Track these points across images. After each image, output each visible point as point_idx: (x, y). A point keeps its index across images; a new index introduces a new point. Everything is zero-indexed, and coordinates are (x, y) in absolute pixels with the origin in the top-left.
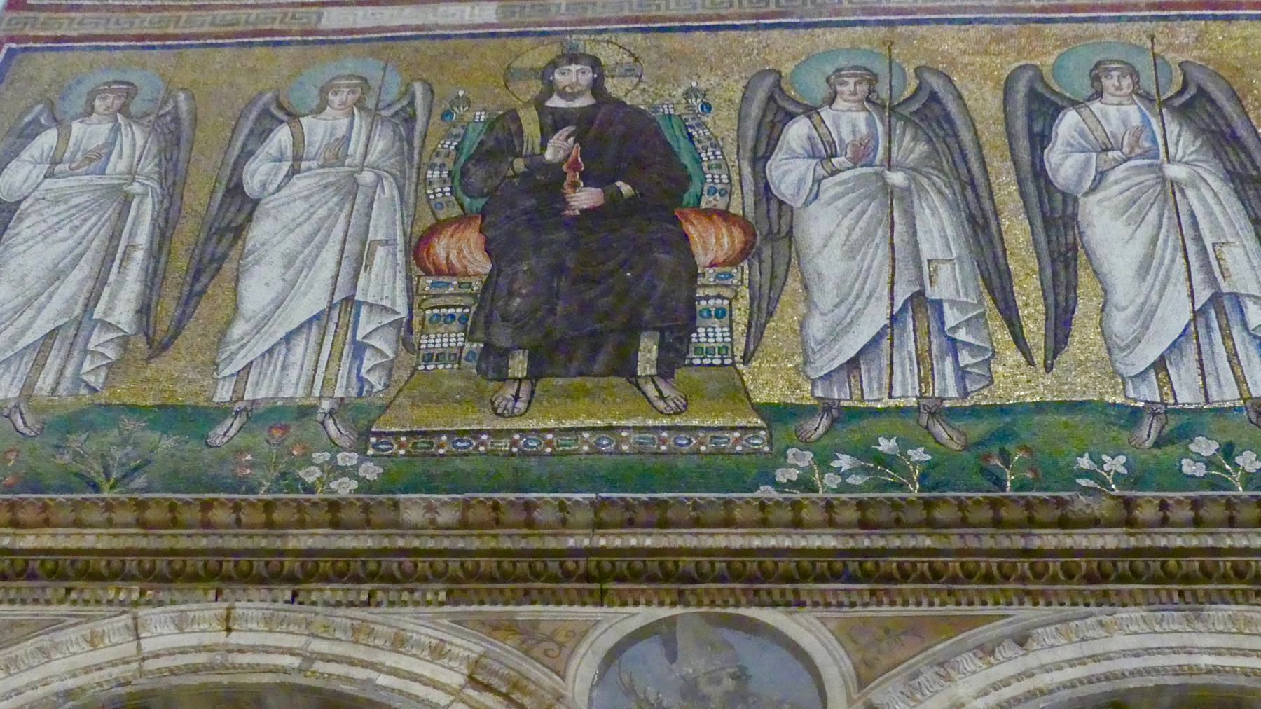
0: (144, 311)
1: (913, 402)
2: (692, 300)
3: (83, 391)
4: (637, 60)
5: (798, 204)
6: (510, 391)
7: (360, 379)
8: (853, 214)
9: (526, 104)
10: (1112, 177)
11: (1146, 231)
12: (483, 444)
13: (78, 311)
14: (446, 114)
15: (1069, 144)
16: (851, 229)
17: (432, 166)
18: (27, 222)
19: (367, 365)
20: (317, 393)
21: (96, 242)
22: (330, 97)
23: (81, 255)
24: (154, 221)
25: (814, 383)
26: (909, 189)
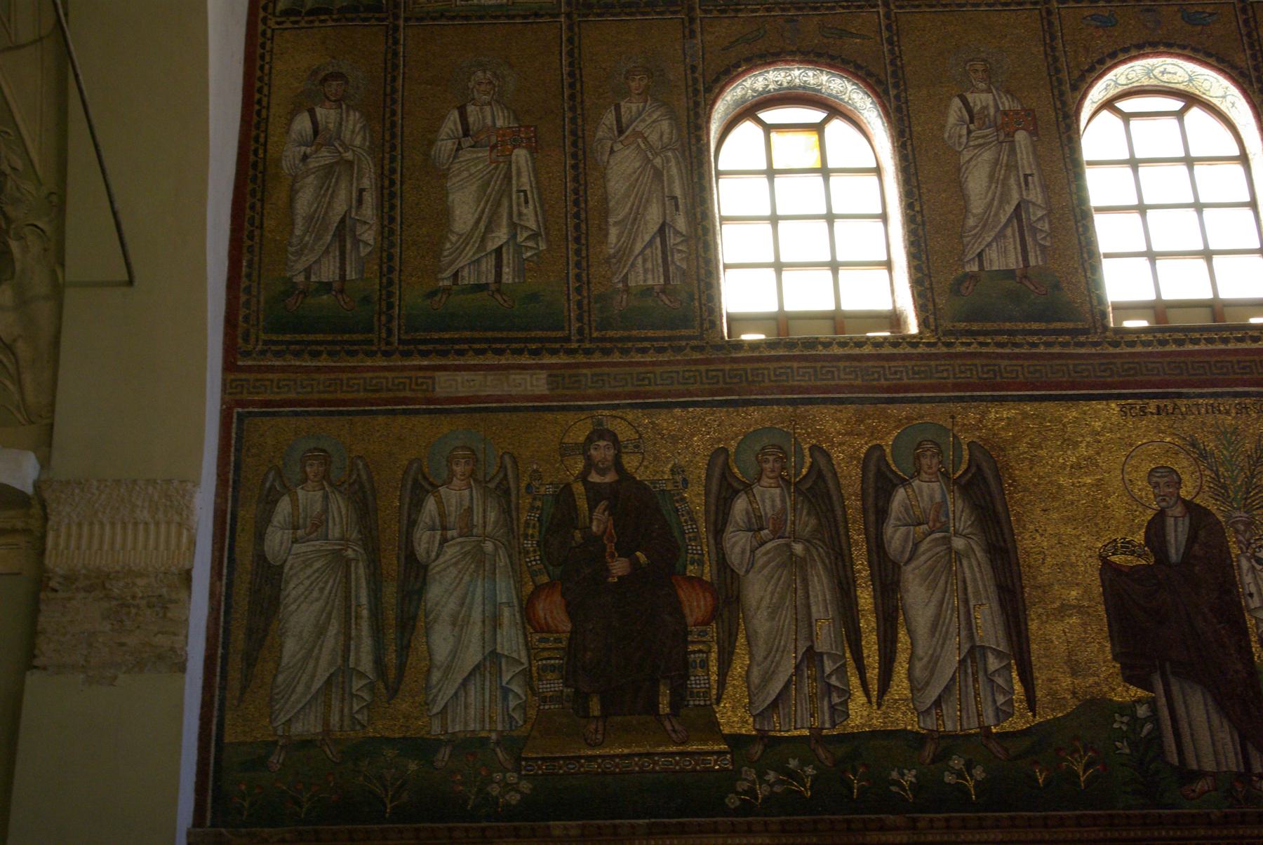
0: (378, 662)
1: (807, 733)
2: (687, 653)
3: (358, 727)
4: (640, 437)
5: (742, 573)
6: (592, 727)
7: (511, 717)
8: (773, 581)
9: (575, 481)
10: (924, 546)
11: (937, 595)
12: (582, 766)
13: (340, 661)
14: (529, 486)
15: (899, 519)
16: (772, 593)
17: (526, 536)
18: (292, 585)
19: (512, 704)
20: (487, 727)
21: (337, 603)
22: (454, 467)
23: (330, 614)
24: (368, 582)
25: (755, 717)
26: (803, 559)
